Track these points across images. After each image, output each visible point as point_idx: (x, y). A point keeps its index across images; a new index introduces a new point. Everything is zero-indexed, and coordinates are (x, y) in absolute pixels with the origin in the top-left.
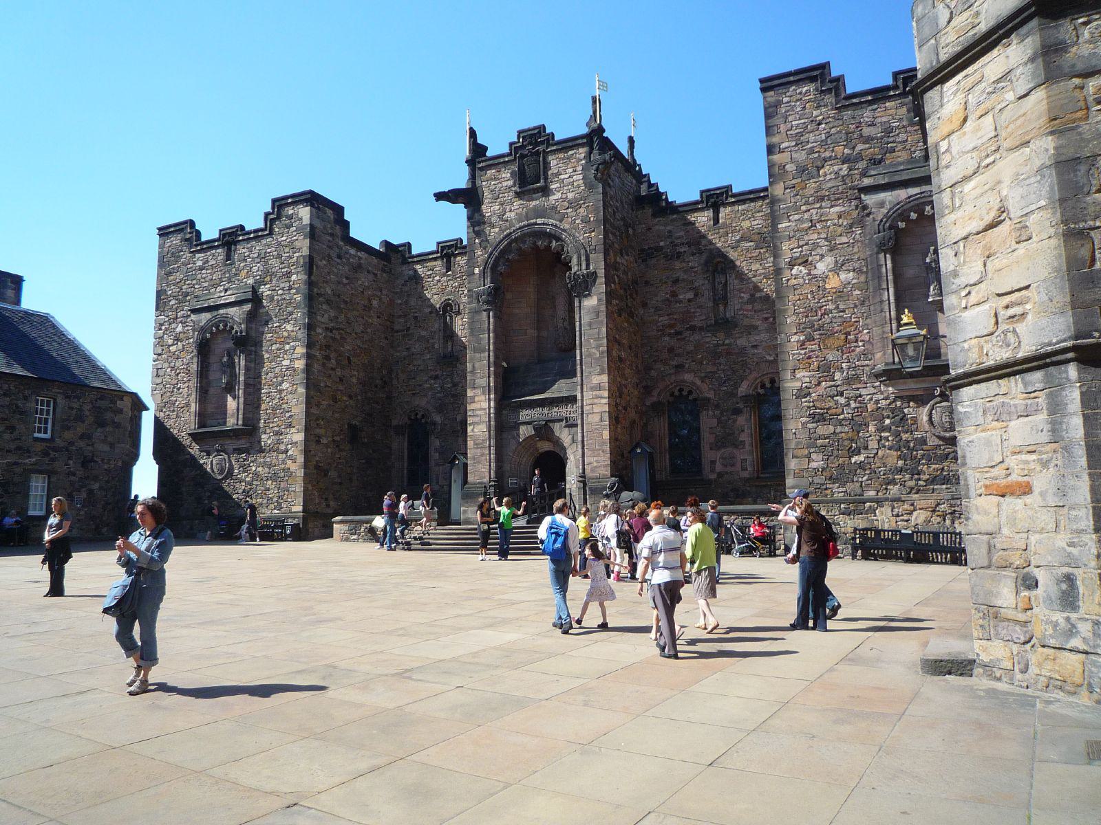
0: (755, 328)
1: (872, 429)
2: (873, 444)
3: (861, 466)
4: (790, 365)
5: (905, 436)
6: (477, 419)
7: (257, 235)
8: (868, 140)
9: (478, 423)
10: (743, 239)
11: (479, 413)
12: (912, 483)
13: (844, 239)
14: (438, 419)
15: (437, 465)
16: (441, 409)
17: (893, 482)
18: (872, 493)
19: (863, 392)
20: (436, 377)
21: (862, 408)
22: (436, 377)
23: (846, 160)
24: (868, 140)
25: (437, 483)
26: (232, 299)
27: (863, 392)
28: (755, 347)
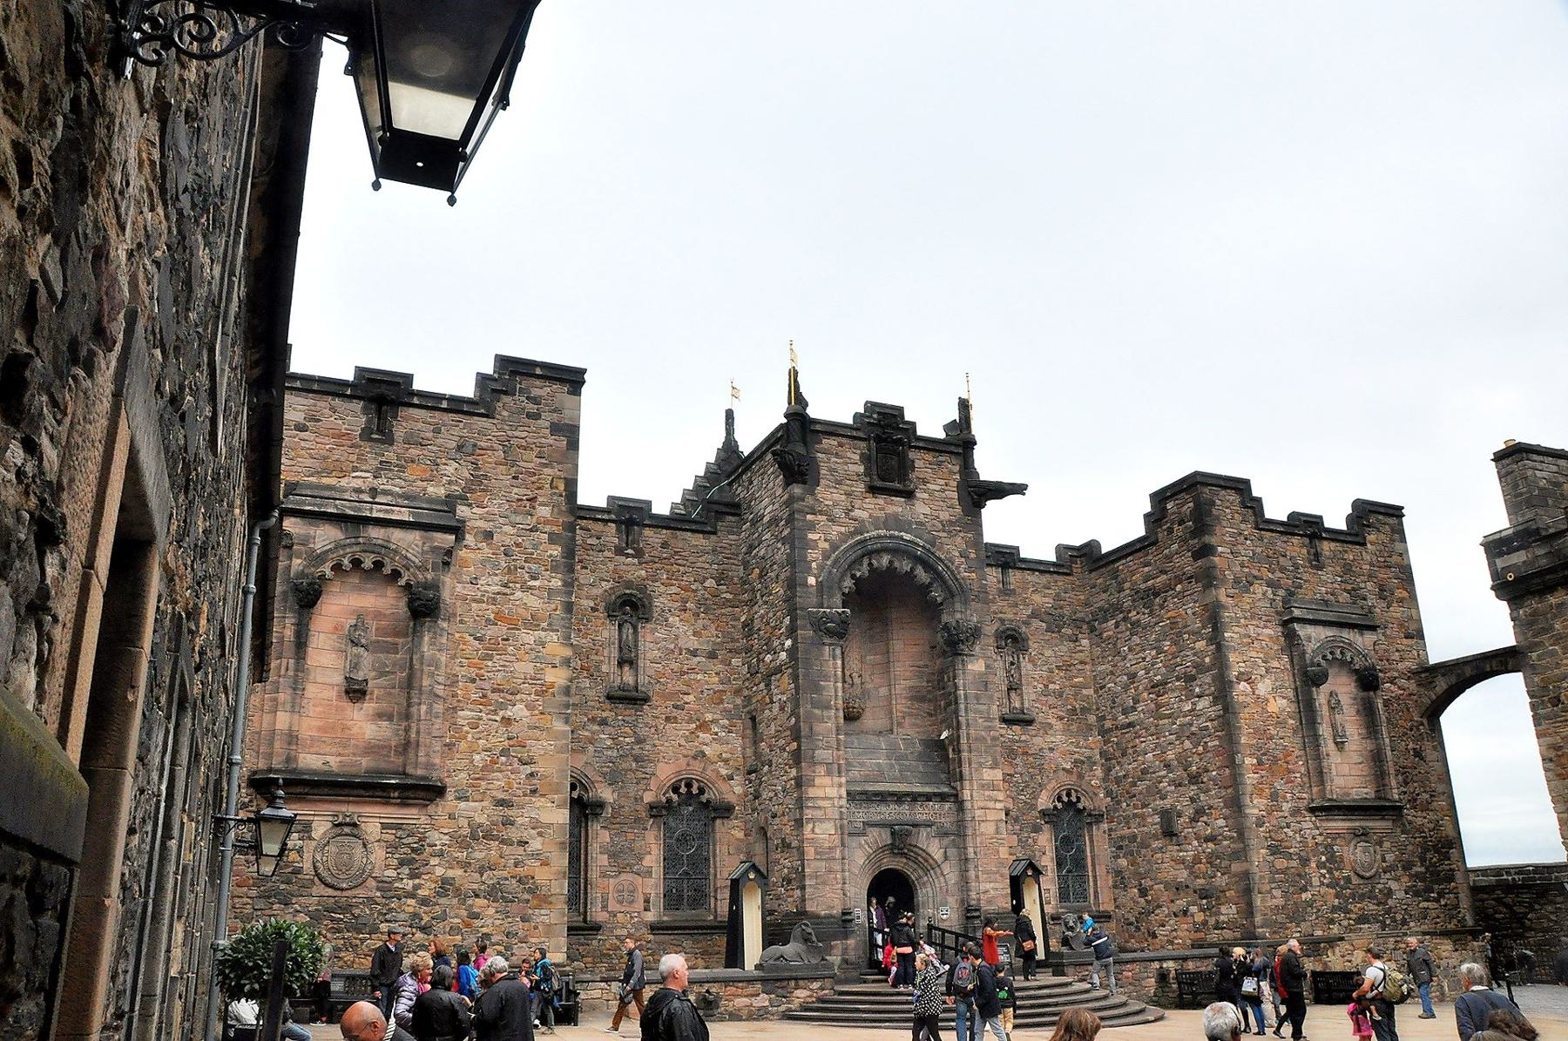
0: (1050, 726)
1: (1313, 865)
2: (1315, 881)
3: (1310, 904)
4: (1249, 789)
5: (1336, 874)
6: (819, 813)
7: (456, 405)
8: (1283, 570)
9: (821, 821)
10: (1034, 615)
11: (821, 803)
12: (1345, 923)
13: (1275, 664)
14: (606, 794)
15: (604, 875)
16: (613, 779)
17: (1332, 921)
18: (1320, 933)
19: (1305, 825)
20: (604, 722)
21: (1304, 842)
22: (604, 722)
24: (1283, 570)
25: (604, 907)
26: (404, 515)
27: (1305, 825)
28: (1051, 749)
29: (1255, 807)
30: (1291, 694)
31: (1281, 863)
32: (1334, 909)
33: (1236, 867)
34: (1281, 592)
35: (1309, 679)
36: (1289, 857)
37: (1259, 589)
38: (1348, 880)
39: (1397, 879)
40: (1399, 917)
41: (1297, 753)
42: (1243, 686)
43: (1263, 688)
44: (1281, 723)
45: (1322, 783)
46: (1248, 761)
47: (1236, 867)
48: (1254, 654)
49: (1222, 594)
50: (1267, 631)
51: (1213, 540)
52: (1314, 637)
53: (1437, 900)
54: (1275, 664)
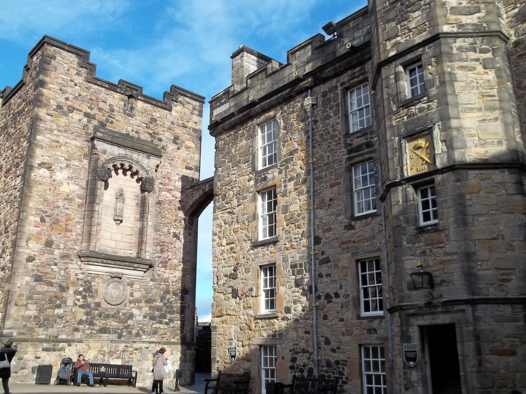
2: (70, 302)
3: (61, 317)
5: (89, 300)
8: (100, 109)
17: (77, 330)
21: (67, 277)
23: (86, 115)
24: (100, 109)
29: (31, 247)
30: (84, 184)
31: (42, 288)
32: (81, 322)
33: (7, 287)
34: (95, 122)
35: (99, 176)
36: (51, 284)
37: (76, 116)
38: (98, 305)
39: (140, 308)
40: (134, 332)
41: (77, 220)
42: (43, 172)
43: (60, 175)
44: (68, 199)
45: (89, 241)
46: (32, 218)
47: (7, 287)
48: (59, 153)
49: (42, 112)
50: (74, 142)
51: (47, 79)
52: (108, 151)
53: (167, 324)
54: (76, 163)
